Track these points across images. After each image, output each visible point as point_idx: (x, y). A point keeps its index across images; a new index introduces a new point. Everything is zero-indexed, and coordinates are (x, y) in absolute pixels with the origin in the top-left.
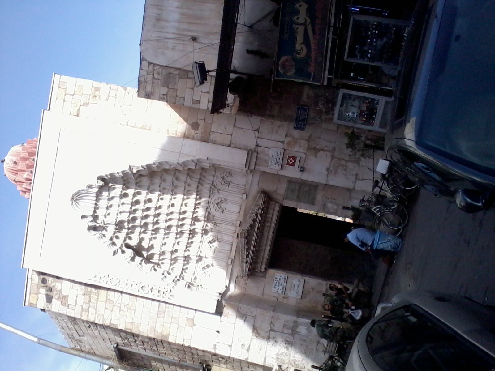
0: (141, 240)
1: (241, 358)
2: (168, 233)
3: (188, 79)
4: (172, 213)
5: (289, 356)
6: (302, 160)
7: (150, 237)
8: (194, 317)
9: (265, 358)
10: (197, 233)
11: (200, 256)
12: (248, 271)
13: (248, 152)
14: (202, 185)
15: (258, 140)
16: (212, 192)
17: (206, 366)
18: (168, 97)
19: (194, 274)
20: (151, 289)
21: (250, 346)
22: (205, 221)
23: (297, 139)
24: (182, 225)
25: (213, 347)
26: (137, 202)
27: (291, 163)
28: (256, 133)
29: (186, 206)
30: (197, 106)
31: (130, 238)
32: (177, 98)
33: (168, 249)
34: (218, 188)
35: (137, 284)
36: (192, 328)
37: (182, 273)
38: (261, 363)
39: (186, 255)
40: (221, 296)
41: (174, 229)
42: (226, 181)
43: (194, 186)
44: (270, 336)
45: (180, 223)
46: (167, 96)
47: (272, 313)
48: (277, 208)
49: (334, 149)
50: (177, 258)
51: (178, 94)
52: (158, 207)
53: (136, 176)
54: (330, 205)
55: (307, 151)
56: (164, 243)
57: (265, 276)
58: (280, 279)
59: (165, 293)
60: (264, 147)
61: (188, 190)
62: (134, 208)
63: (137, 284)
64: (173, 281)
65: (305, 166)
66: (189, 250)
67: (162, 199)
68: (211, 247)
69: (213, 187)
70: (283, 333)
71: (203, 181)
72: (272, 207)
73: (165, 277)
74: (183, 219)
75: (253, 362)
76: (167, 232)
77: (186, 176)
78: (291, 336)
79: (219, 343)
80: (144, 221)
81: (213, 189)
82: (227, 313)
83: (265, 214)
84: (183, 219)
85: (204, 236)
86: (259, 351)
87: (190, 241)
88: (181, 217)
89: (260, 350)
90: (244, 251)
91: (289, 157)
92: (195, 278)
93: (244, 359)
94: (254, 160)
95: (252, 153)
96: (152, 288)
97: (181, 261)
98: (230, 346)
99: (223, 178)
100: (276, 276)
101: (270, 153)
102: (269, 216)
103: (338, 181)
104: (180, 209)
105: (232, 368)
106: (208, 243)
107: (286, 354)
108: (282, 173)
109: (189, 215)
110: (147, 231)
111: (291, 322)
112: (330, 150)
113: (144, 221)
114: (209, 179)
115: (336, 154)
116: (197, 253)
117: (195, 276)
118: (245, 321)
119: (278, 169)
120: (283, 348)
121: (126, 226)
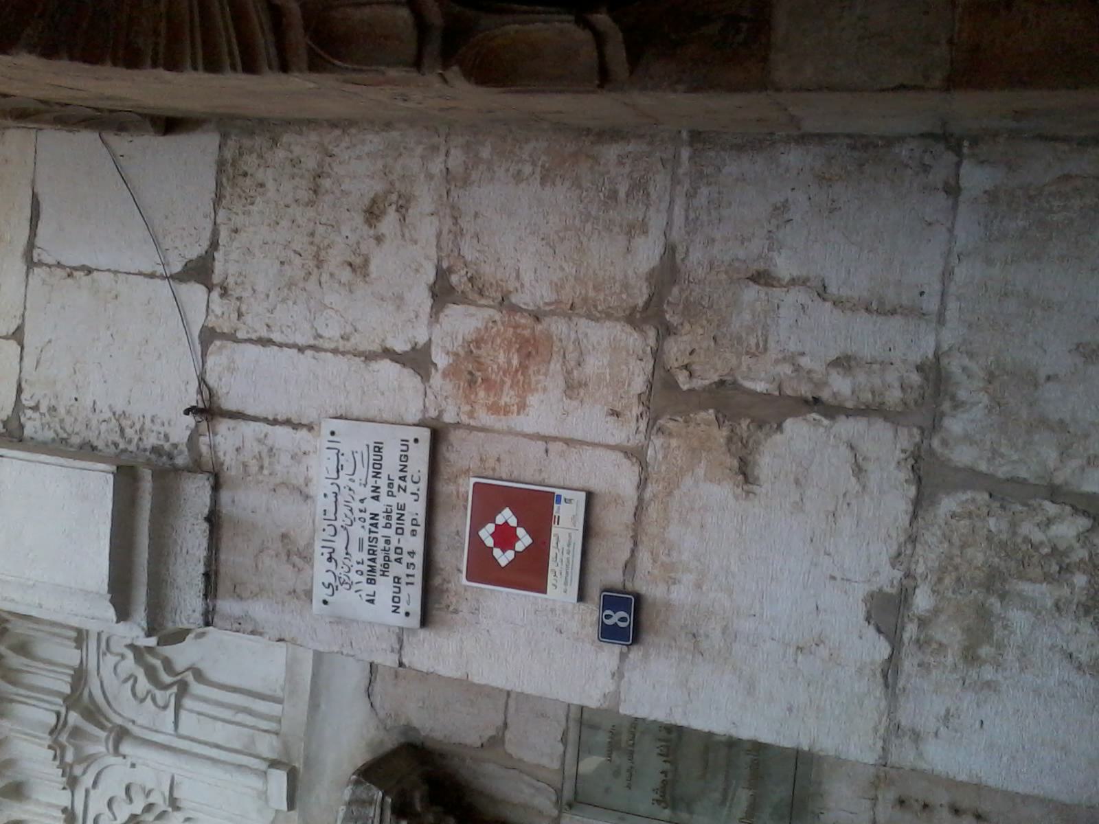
6: (615, 520)
13: (126, 477)
16: (78, 750)
34: (119, 721)
55: (653, 425)
60: (266, 420)
65: (641, 585)
69: (74, 718)
81: (76, 732)
94: (192, 540)
112: (894, 396)
115: (965, 437)
119: (398, 620)
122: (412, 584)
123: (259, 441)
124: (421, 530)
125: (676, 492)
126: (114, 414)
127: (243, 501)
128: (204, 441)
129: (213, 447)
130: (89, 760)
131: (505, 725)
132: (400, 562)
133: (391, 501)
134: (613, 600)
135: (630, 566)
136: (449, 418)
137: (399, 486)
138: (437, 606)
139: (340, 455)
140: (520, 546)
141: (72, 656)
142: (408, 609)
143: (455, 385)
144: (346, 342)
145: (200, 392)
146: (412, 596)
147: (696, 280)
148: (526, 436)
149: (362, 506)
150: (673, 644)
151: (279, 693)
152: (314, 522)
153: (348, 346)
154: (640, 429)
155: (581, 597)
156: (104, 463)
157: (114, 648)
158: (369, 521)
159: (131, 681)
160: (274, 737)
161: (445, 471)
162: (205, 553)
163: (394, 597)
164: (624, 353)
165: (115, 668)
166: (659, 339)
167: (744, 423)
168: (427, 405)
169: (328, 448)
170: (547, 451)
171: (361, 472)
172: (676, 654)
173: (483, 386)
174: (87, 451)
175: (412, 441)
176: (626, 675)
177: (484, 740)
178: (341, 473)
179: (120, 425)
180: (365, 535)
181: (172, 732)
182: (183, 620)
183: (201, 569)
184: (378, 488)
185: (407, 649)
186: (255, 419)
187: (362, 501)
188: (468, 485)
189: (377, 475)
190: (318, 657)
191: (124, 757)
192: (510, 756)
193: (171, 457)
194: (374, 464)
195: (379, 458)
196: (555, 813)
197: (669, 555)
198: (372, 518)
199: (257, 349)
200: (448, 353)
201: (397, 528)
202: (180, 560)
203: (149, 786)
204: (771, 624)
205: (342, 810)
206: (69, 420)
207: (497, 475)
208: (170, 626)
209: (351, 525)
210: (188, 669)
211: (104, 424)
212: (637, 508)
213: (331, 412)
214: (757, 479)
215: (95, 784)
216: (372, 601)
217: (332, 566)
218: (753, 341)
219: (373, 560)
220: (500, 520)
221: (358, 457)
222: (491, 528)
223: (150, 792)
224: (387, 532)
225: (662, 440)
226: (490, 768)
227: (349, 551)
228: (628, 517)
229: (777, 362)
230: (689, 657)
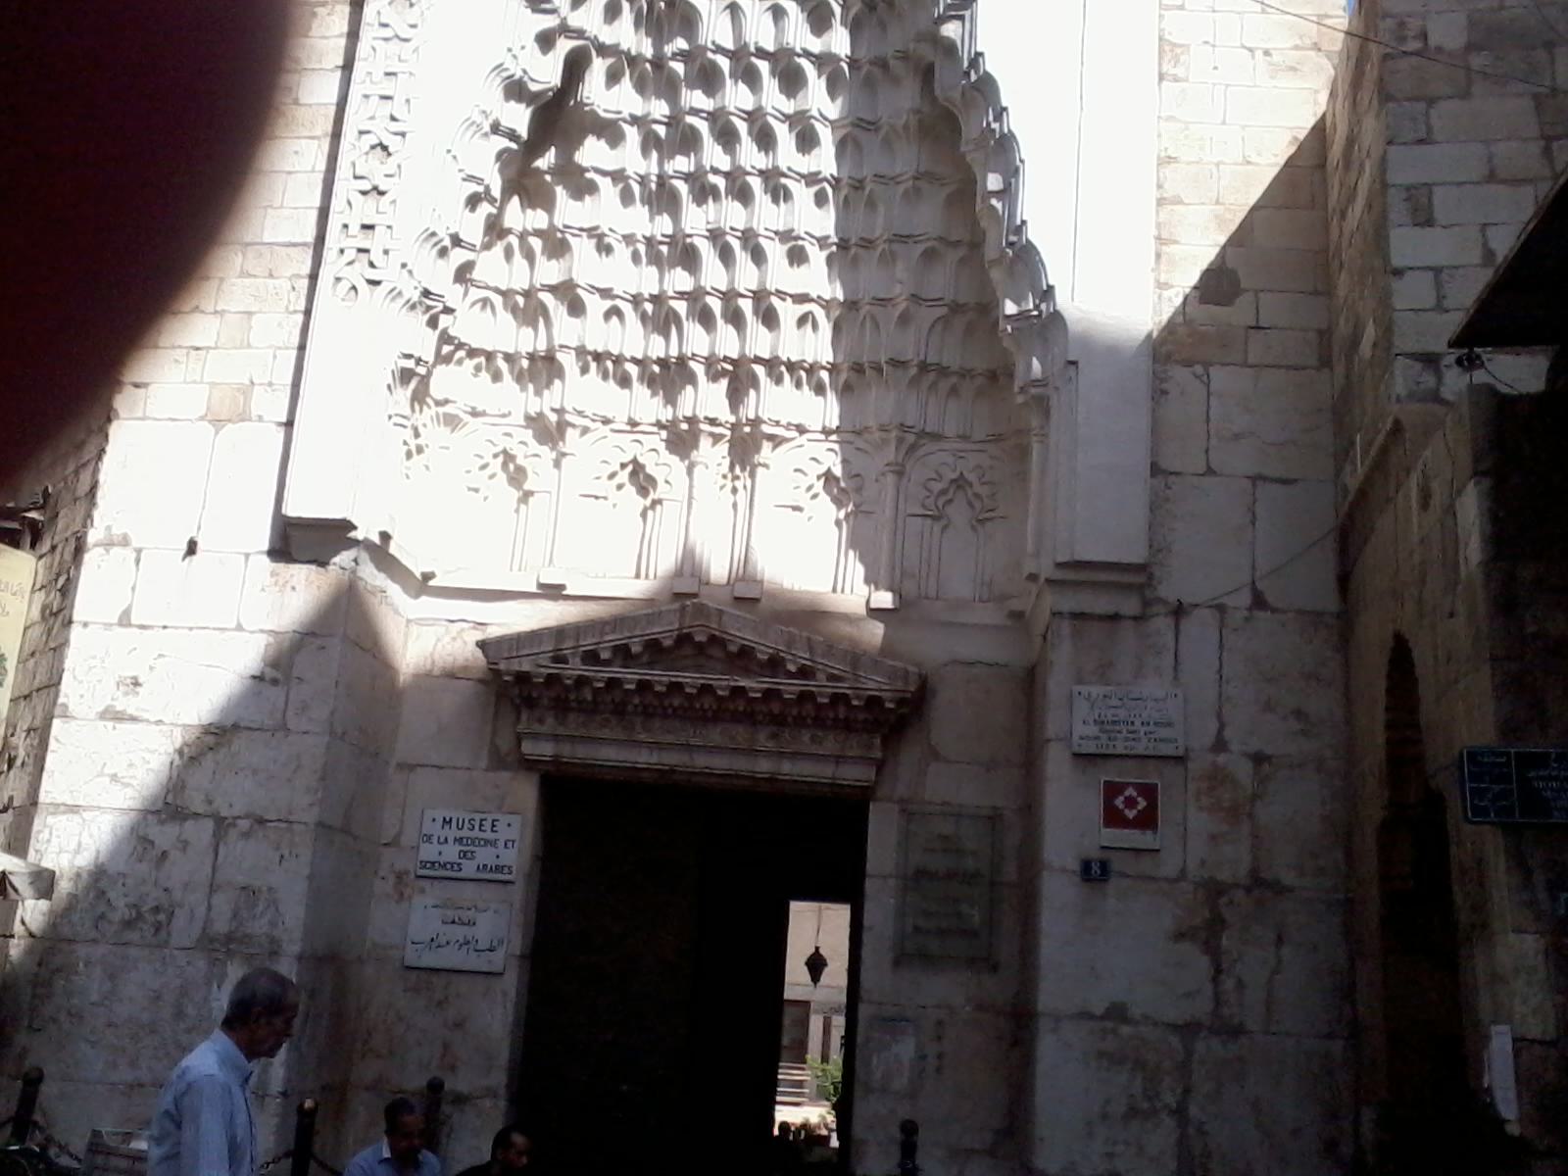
0: (610, 130)
1: (66, 677)
2: (655, 259)
3: (1542, 143)
4: (758, 256)
5: (93, 934)
7: (630, 172)
8: (260, 419)
9: (74, 809)
10: (671, 400)
11: (562, 426)
12: (515, 666)
14: (914, 382)
15: (1207, 611)
17: (33, 523)
18: (1414, 60)
19: (475, 414)
20: (375, 188)
21: (133, 719)
22: (734, 427)
23: (1250, 816)
24: (706, 318)
25: (117, 531)
26: (791, 81)
27: (1119, 802)
28: (1245, 599)
29: (802, 321)
30: (1398, 210)
31: (613, 77)
32: (1421, 106)
34: (908, 467)
35: (393, 119)
36: (202, 418)
37: (472, 353)
38: (49, 791)
39: (559, 356)
40: (376, 539)
41: (680, 280)
42: (950, 501)
43: (909, 346)
44: (189, 824)
45: (715, 305)
46: (1417, 53)
47: (311, 817)
48: (853, 774)
49: (1236, 1032)
50: (541, 321)
51: (1444, 106)
52: (783, 180)
53: (926, 52)
54: (905, 1049)
56: (607, 240)
57: (498, 762)
58: (493, 843)
59: (364, 257)
62: (763, 66)
63: (393, 119)
64: (426, 293)
66: (584, 370)
67: (820, 200)
68: (612, 476)
69: (911, 438)
70: (213, 888)
71: (933, 386)
73: (443, 252)
74: (735, 318)
75: (52, 744)
76: (664, 249)
77: (949, 297)
78: (196, 932)
79: (138, 561)
80: (702, 126)
82: (294, 582)
83: (816, 719)
84: (735, 318)
85: (664, 434)
86: (106, 771)
87: (633, 370)
88: (746, 305)
89: (114, 778)
90: (613, 638)
92: (452, 422)
93: (61, 700)
94: (1102, 604)
95: (1140, 588)
96: (382, 193)
97: (526, 341)
98: (125, 620)
99: (960, 483)
100: (504, 819)
101: (1154, 687)
102: (806, 737)
103: (1065, 1078)
104: (781, 294)
105: (27, 650)
106: (635, 461)
107: (102, 917)
108: (1056, 764)
109: (759, 341)
110: (655, 155)
111: (273, 924)
112: (1226, 1011)
113: (702, 126)
114: (949, 416)
115: (1207, 1047)
116: (580, 413)
117: (467, 418)
118: (258, 678)
120: (131, 900)
121: (668, 49)
127: (1127, 632)
133: (1142, 733)
136: (1190, 765)
146: (1090, 748)
159: (934, 476)
189: (1155, 724)
222: (1135, 794)
224: (1125, 731)
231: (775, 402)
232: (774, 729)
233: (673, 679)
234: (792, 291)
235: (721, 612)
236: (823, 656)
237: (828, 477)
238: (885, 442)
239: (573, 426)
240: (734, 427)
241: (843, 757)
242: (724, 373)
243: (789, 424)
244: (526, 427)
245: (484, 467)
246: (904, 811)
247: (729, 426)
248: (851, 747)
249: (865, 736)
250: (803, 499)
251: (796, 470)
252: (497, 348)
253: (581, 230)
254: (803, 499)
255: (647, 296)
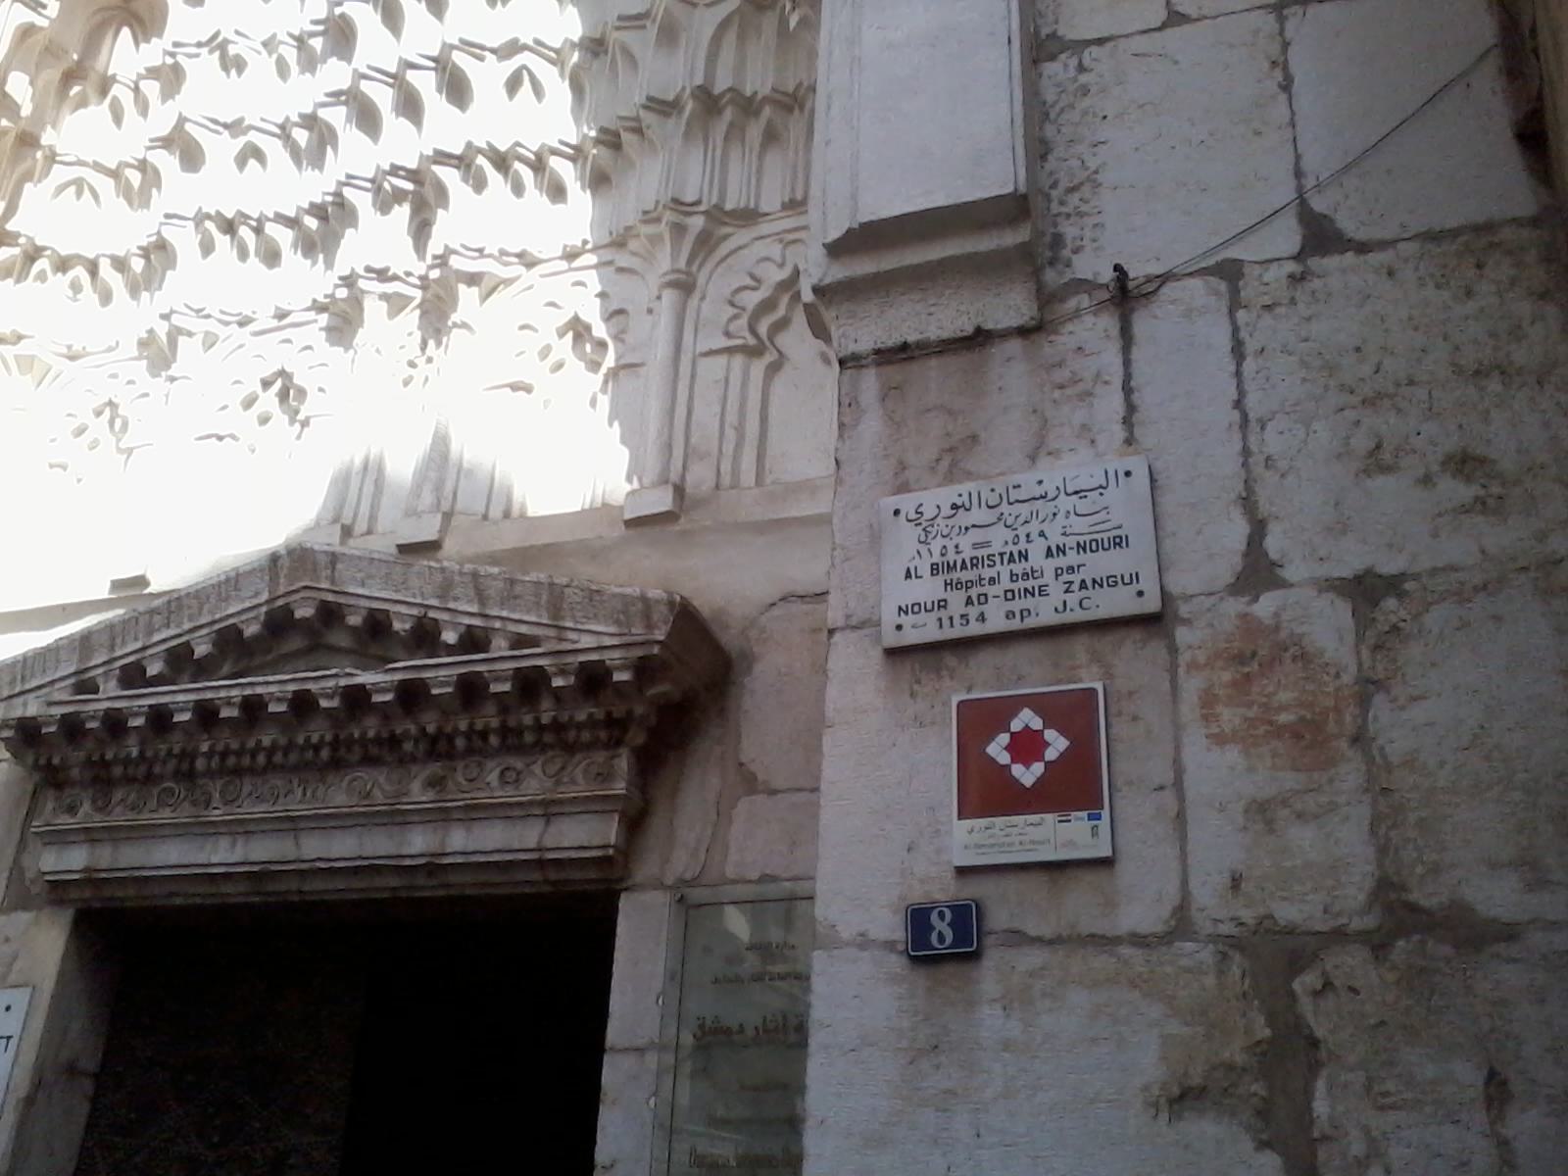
6: (1079, 907)
12: (18, 713)
13: (1015, 208)
15: (1196, 283)
23: (1359, 739)
28: (1286, 237)
29: (513, 85)
33: (207, 92)
34: (701, 280)
37: (63, 265)
41: (336, 74)
43: (672, 73)
48: (584, 834)
55: (1229, 945)
60: (1128, 377)
61: (636, 50)
65: (993, 958)
66: (207, 248)
68: (249, 403)
69: (697, 223)
71: (735, 132)
72: (579, 783)
74: (410, 106)
83: (504, 731)
87: (283, 236)
88: (425, 83)
90: (165, 634)
91: (1074, 712)
94: (946, 315)
102: (493, 777)
109: (446, 127)
119: (889, 616)
122: (941, 626)
123: (1098, 375)
124: (1015, 624)
125: (1137, 994)
126: (1096, 172)
127: (1011, 373)
128: (1084, 300)
129: (1077, 314)
130: (648, 258)
131: (773, 792)
132: (967, 604)
134: (966, 919)
135: (1017, 938)
136: (1182, 635)
137: (1071, 583)
138: (917, 666)
139: (1101, 490)
140: (1017, 770)
141: (770, 202)
142: (907, 628)
143: (1233, 634)
144: (1263, 464)
145: (1149, 279)
146: (926, 630)
147: (1469, 981)
148: (1178, 749)
149: (1034, 535)
150: (920, 1017)
151: (768, 481)
152: (1002, 474)
153: (1258, 469)
154: (1221, 925)
155: (962, 871)
156: (1027, 180)
157: (791, 248)
158: (1015, 550)
160: (713, 485)
161: (1105, 643)
162: (933, 337)
163: (919, 604)
164: (1330, 882)
165: (767, 259)
166: (1363, 936)
167: (1258, 1088)
168: (1195, 600)
169: (1106, 472)
170: (1162, 788)
171: (1080, 525)
172: (906, 1024)
173: (1238, 676)
174: (1038, 150)
175: (1140, 587)
176: (865, 954)
177: (753, 768)
178: (1075, 497)
179: (1082, 184)
180: (996, 548)
181: (698, 351)
182: (841, 331)
183: (912, 338)
184: (1064, 553)
185: (853, 635)
186: (1127, 363)
187: (1042, 534)
188: (1092, 681)
189: (1081, 547)
190: (823, 520)
191: (659, 298)
192: (733, 807)
193: (1052, 263)
194: (1097, 541)
195: (1106, 545)
196: (669, 880)
197: (1044, 995)
198: (1020, 552)
199: (1224, 342)
200: (1276, 615)
201: (1013, 591)
202: (919, 307)
203: (627, 337)
204: (971, 1162)
205: (633, 591)
206: (1074, 116)
207: (1114, 721)
208: (828, 315)
209: (1006, 526)
210: (778, 351)
211: (1079, 163)
212: (1103, 937)
213: (1158, 465)
214: (1180, 1118)
215: (621, 270)
216: (908, 575)
217: (947, 511)
218: (1390, 1086)
219: (964, 566)
220: (1050, 735)
221: (1102, 516)
222: (1037, 723)
223: (622, 341)
224: (1005, 577)
225: (1210, 961)
226: (714, 781)
227: (971, 530)
228: (1087, 927)
229: (1366, 1130)
230: (904, 1044)
231: (472, 219)
232: (435, 768)
233: (248, 692)
234: (495, 45)
235: (334, 558)
236: (502, 605)
237: (578, 330)
238: (655, 240)
239: (190, 334)
240: (425, 283)
241: (561, 802)
242: (399, 196)
243: (503, 253)
244: (139, 358)
245: (80, 431)
246: (681, 900)
247: (413, 280)
248: (573, 782)
249: (600, 756)
250: (535, 372)
251: (522, 327)
252: (100, 252)
253: (199, 45)
254: (535, 372)
255: (295, 118)
